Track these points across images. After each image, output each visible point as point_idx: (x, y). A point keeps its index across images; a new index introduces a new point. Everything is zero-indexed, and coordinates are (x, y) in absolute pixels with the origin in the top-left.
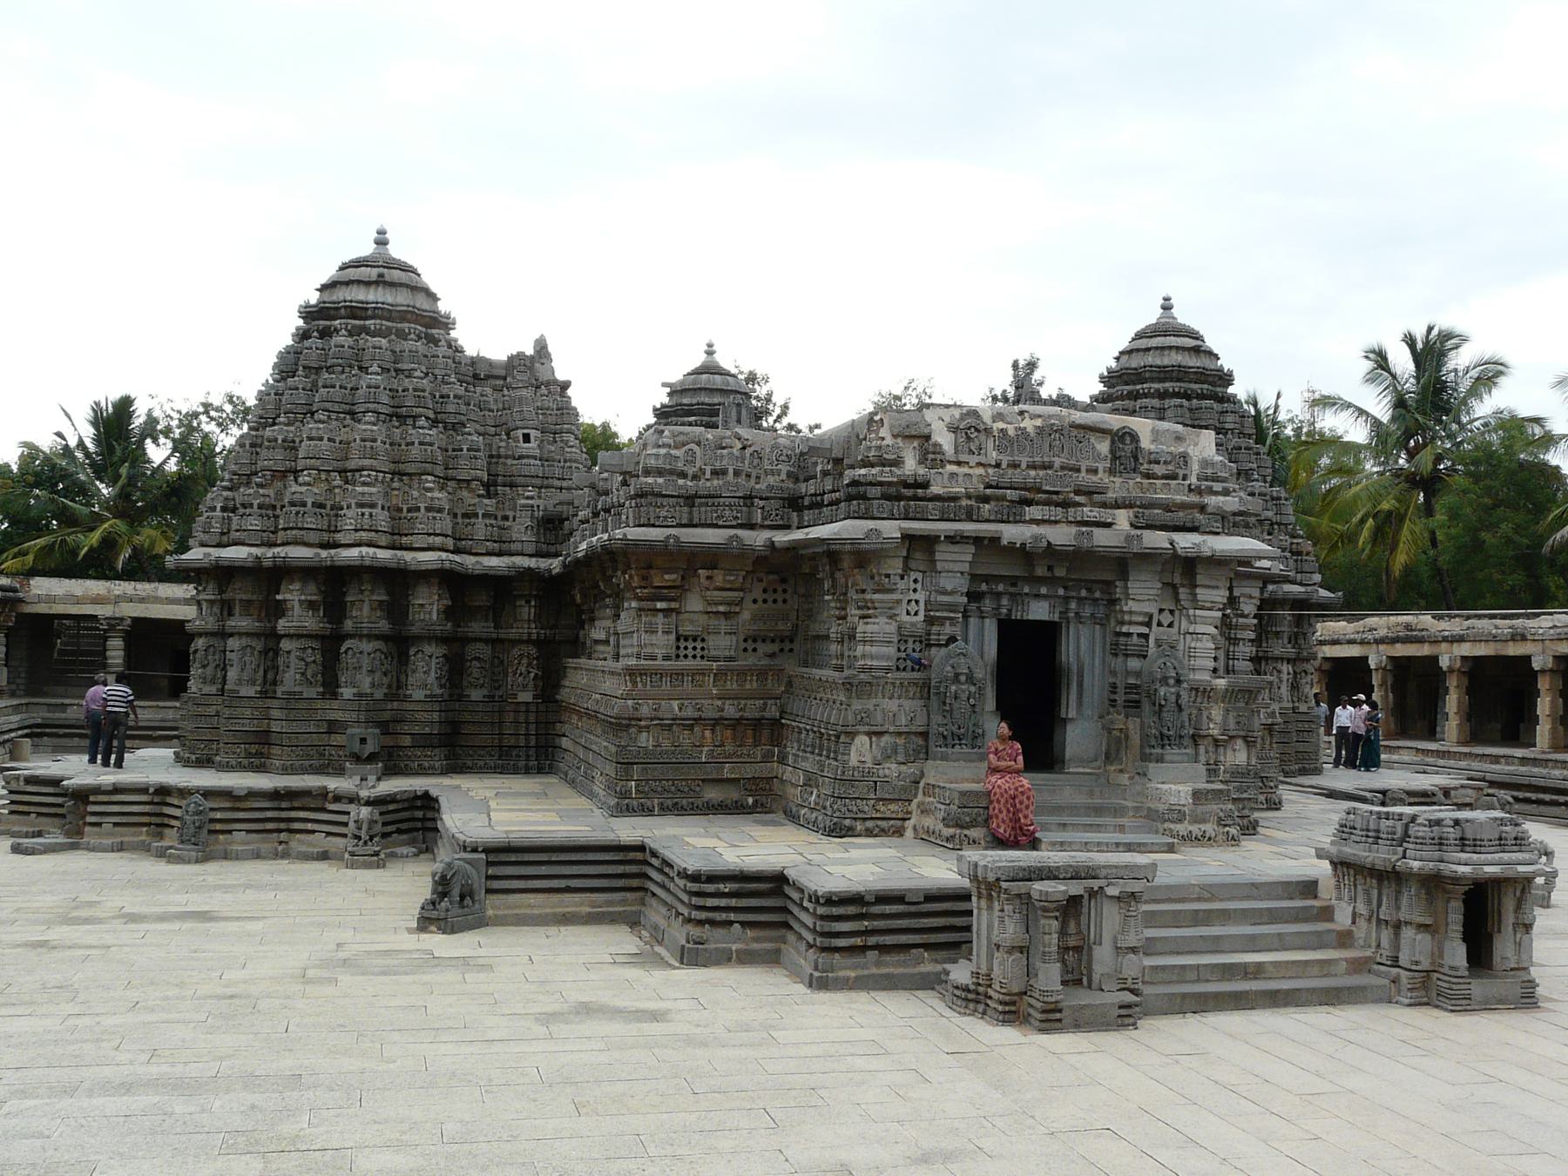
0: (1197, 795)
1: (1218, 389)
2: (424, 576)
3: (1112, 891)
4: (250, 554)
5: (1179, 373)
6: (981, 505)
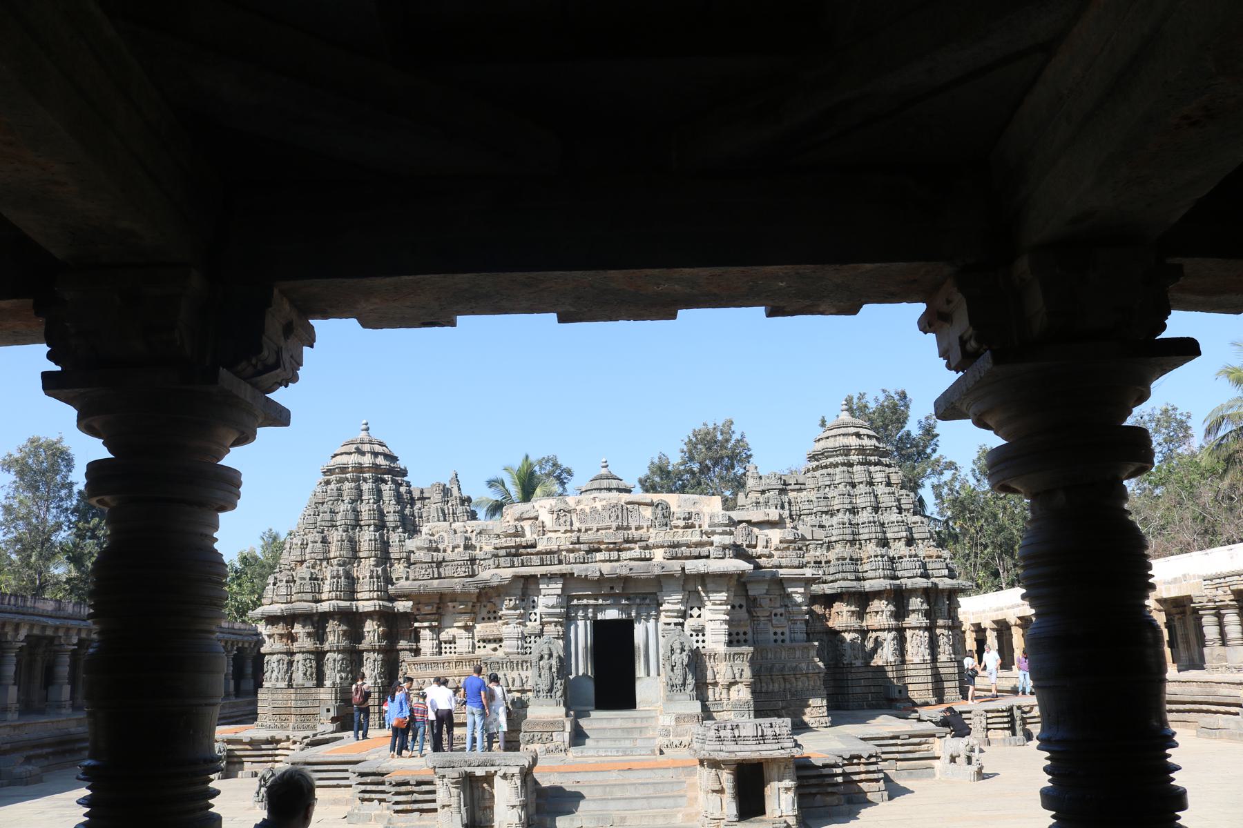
0: (678, 719)
1: (872, 458)
2: (369, 615)
3: (500, 773)
4: (279, 608)
5: (846, 451)
6: (567, 555)
